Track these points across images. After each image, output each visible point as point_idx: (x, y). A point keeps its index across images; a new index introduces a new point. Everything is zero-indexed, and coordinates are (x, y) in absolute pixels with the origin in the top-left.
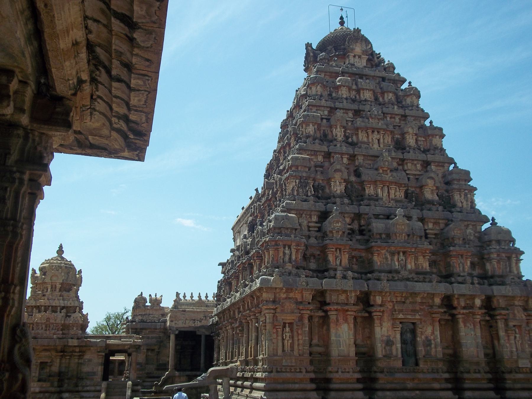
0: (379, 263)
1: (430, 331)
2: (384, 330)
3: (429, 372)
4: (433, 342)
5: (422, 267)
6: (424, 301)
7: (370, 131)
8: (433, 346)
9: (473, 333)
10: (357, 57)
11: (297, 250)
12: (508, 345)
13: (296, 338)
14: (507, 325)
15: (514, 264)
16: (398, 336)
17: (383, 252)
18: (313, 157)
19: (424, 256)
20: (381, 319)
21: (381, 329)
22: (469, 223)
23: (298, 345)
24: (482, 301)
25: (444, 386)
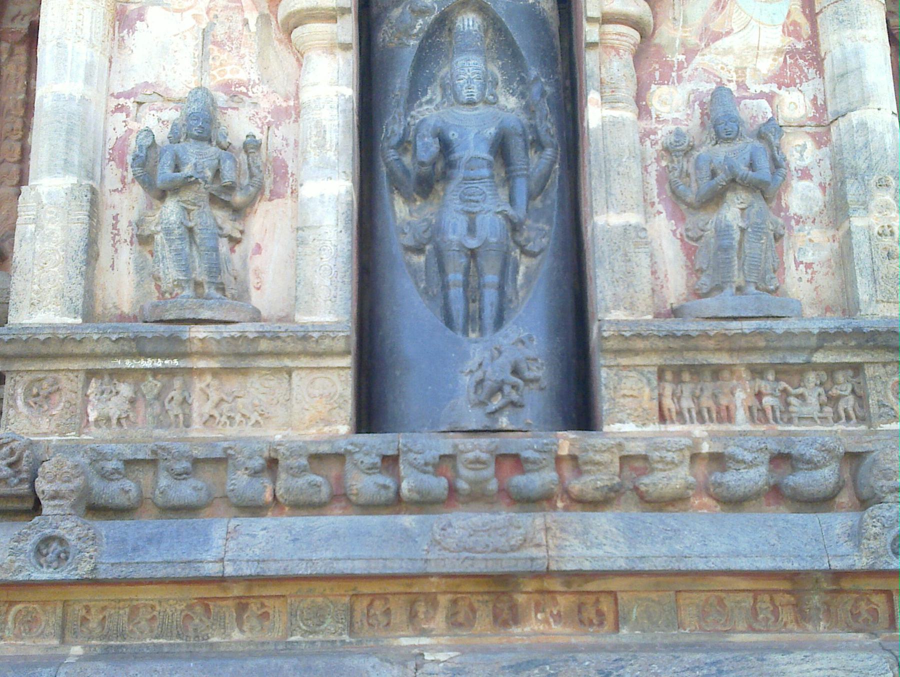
3: (734, 502)
4: (799, 150)
8: (802, 196)
16: (329, 82)
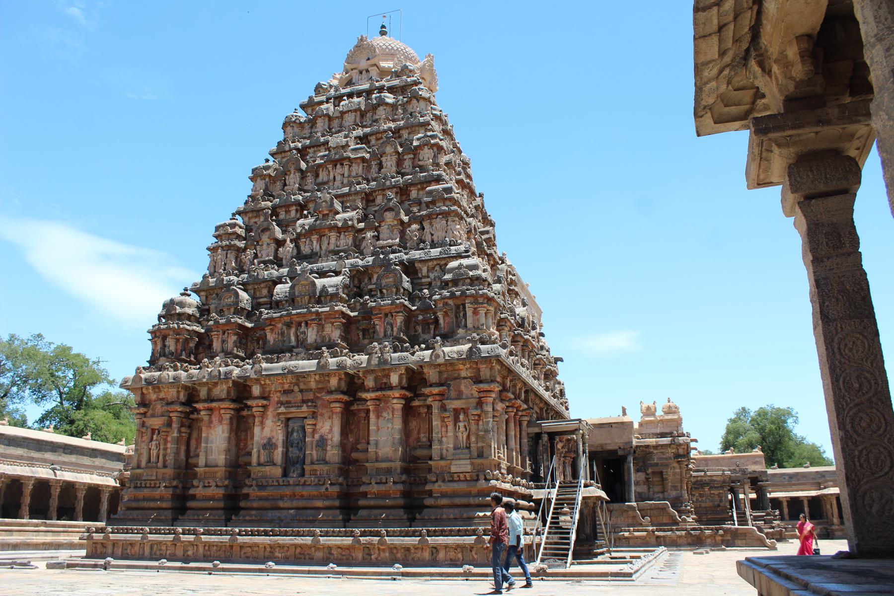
0: (272, 342)
1: (328, 428)
2: (268, 430)
4: (329, 442)
5: (330, 339)
6: (320, 386)
7: (330, 167)
8: (329, 448)
9: (390, 425)
10: (364, 72)
11: (178, 340)
12: (444, 439)
13: (162, 447)
14: (443, 408)
15: (469, 313)
17: (280, 325)
18: (256, 220)
19: (332, 324)
20: (263, 415)
21: (263, 428)
22: (435, 263)
23: (165, 456)
24: (401, 375)
25: (327, 503)
